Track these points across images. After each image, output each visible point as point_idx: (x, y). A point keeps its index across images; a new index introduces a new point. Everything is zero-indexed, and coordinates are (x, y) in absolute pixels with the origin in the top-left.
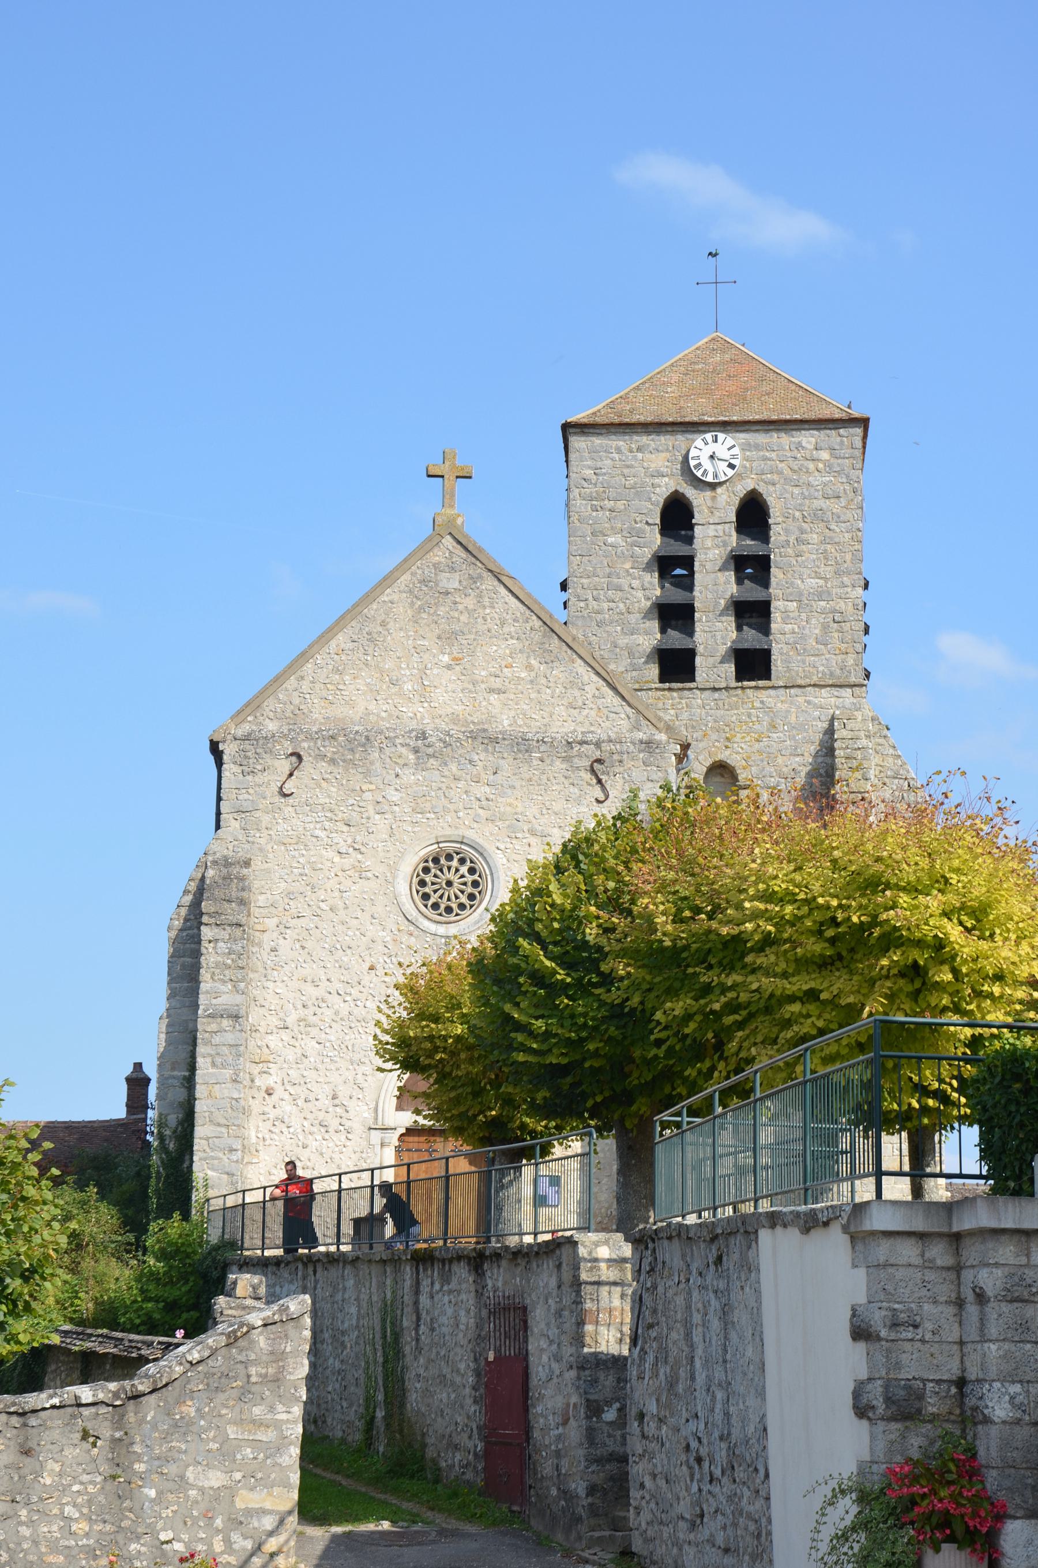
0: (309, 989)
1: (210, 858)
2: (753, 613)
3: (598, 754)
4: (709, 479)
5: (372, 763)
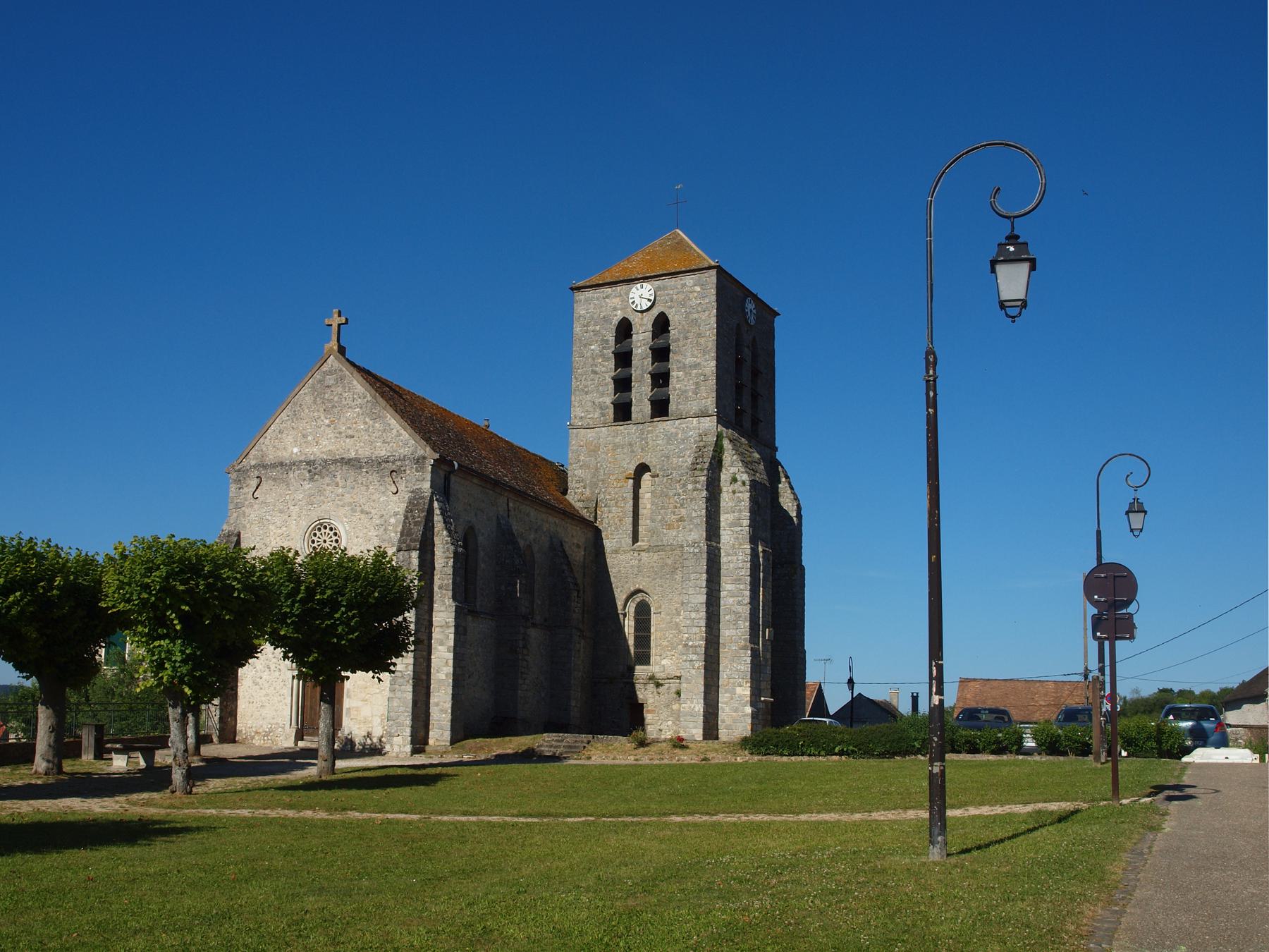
2: (661, 379)
3: (394, 467)
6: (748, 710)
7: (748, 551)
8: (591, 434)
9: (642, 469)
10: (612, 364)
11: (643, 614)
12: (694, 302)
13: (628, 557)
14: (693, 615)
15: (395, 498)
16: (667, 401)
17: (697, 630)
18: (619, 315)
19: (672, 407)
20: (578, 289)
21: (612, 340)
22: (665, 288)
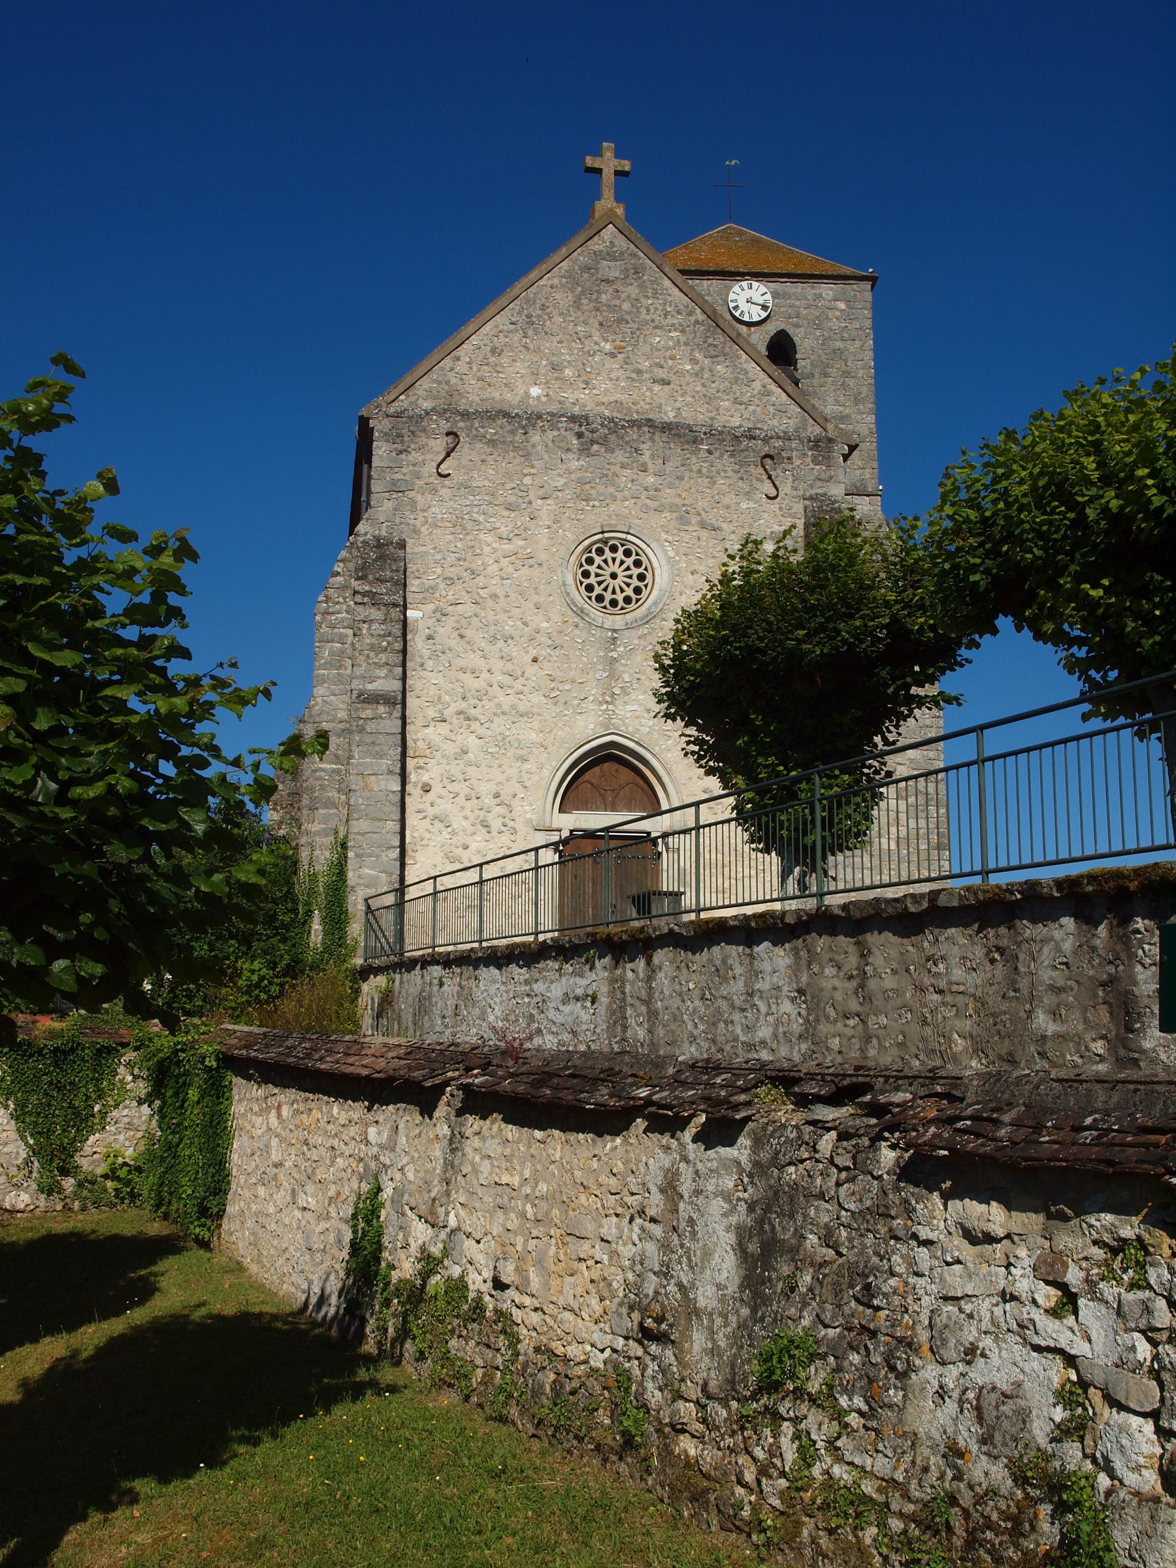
0: (467, 679)
1: (361, 539)
4: (746, 318)
5: (534, 446)
15: (773, 506)
22: (785, 296)
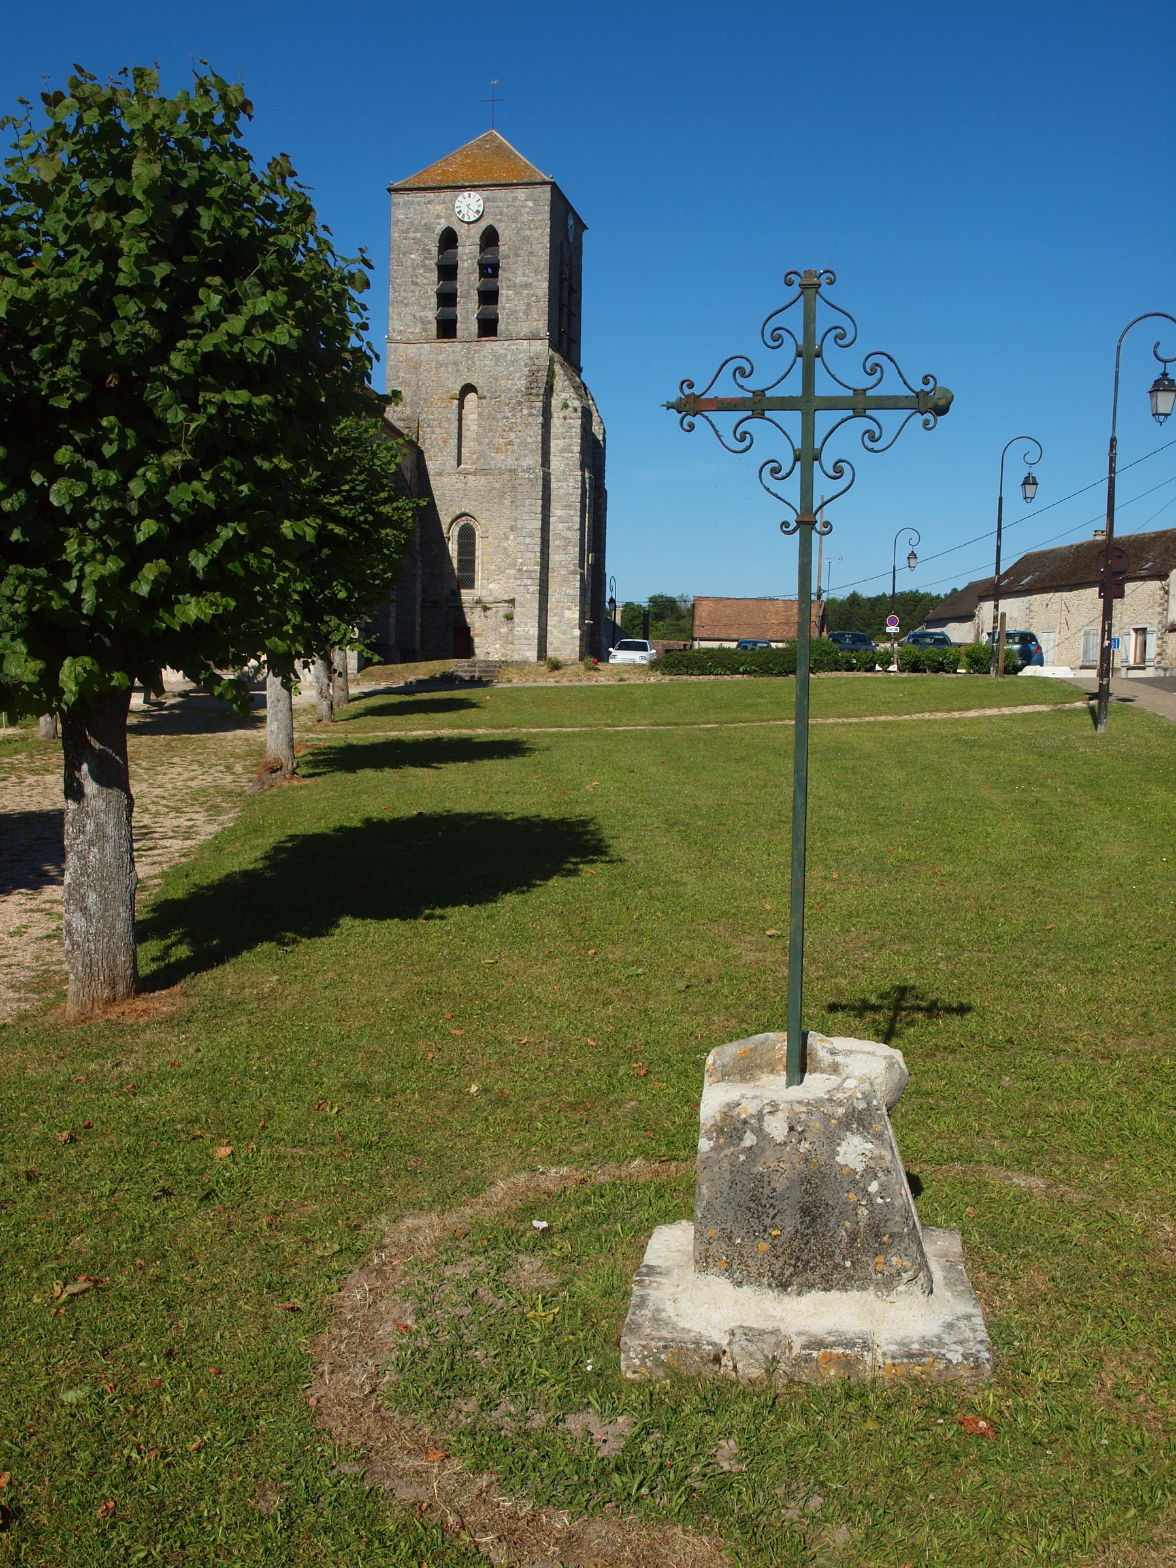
2: (489, 297)
4: (466, 219)
6: (577, 632)
7: (579, 478)
8: (411, 349)
9: (468, 389)
10: (434, 276)
11: (467, 537)
12: (526, 218)
13: (453, 479)
14: (528, 540)
16: (496, 321)
17: (532, 555)
18: (443, 224)
19: (501, 327)
20: (397, 190)
21: (435, 250)
22: (494, 200)
